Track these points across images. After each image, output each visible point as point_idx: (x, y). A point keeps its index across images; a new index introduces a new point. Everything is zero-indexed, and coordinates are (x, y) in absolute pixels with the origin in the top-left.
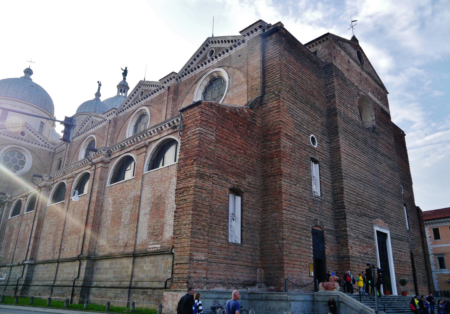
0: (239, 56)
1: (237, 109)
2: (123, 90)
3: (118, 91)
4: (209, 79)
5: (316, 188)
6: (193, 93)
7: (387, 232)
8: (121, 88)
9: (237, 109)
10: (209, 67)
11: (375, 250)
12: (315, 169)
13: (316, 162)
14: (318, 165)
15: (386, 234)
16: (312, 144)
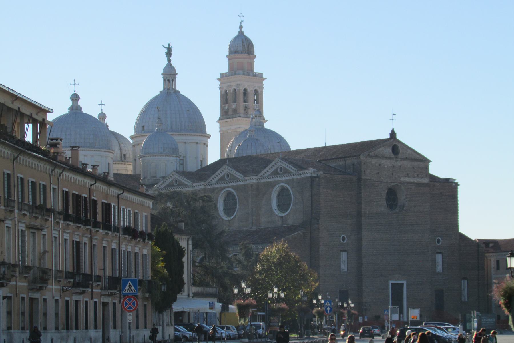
0: (299, 183)
1: (296, 235)
2: (171, 80)
3: (165, 80)
4: (280, 188)
5: (344, 267)
6: (271, 194)
7: (405, 282)
8: (168, 78)
9: (296, 235)
10: (280, 181)
11: (389, 295)
12: (344, 256)
13: (344, 251)
14: (346, 253)
15: (403, 284)
16: (342, 241)
